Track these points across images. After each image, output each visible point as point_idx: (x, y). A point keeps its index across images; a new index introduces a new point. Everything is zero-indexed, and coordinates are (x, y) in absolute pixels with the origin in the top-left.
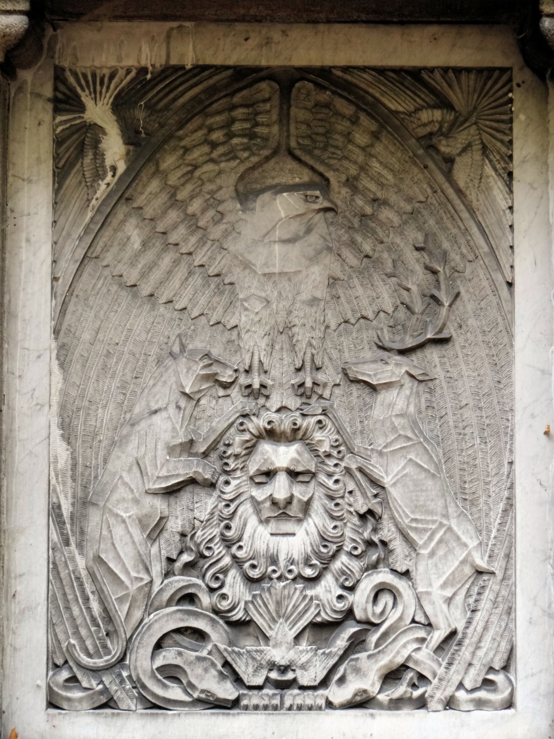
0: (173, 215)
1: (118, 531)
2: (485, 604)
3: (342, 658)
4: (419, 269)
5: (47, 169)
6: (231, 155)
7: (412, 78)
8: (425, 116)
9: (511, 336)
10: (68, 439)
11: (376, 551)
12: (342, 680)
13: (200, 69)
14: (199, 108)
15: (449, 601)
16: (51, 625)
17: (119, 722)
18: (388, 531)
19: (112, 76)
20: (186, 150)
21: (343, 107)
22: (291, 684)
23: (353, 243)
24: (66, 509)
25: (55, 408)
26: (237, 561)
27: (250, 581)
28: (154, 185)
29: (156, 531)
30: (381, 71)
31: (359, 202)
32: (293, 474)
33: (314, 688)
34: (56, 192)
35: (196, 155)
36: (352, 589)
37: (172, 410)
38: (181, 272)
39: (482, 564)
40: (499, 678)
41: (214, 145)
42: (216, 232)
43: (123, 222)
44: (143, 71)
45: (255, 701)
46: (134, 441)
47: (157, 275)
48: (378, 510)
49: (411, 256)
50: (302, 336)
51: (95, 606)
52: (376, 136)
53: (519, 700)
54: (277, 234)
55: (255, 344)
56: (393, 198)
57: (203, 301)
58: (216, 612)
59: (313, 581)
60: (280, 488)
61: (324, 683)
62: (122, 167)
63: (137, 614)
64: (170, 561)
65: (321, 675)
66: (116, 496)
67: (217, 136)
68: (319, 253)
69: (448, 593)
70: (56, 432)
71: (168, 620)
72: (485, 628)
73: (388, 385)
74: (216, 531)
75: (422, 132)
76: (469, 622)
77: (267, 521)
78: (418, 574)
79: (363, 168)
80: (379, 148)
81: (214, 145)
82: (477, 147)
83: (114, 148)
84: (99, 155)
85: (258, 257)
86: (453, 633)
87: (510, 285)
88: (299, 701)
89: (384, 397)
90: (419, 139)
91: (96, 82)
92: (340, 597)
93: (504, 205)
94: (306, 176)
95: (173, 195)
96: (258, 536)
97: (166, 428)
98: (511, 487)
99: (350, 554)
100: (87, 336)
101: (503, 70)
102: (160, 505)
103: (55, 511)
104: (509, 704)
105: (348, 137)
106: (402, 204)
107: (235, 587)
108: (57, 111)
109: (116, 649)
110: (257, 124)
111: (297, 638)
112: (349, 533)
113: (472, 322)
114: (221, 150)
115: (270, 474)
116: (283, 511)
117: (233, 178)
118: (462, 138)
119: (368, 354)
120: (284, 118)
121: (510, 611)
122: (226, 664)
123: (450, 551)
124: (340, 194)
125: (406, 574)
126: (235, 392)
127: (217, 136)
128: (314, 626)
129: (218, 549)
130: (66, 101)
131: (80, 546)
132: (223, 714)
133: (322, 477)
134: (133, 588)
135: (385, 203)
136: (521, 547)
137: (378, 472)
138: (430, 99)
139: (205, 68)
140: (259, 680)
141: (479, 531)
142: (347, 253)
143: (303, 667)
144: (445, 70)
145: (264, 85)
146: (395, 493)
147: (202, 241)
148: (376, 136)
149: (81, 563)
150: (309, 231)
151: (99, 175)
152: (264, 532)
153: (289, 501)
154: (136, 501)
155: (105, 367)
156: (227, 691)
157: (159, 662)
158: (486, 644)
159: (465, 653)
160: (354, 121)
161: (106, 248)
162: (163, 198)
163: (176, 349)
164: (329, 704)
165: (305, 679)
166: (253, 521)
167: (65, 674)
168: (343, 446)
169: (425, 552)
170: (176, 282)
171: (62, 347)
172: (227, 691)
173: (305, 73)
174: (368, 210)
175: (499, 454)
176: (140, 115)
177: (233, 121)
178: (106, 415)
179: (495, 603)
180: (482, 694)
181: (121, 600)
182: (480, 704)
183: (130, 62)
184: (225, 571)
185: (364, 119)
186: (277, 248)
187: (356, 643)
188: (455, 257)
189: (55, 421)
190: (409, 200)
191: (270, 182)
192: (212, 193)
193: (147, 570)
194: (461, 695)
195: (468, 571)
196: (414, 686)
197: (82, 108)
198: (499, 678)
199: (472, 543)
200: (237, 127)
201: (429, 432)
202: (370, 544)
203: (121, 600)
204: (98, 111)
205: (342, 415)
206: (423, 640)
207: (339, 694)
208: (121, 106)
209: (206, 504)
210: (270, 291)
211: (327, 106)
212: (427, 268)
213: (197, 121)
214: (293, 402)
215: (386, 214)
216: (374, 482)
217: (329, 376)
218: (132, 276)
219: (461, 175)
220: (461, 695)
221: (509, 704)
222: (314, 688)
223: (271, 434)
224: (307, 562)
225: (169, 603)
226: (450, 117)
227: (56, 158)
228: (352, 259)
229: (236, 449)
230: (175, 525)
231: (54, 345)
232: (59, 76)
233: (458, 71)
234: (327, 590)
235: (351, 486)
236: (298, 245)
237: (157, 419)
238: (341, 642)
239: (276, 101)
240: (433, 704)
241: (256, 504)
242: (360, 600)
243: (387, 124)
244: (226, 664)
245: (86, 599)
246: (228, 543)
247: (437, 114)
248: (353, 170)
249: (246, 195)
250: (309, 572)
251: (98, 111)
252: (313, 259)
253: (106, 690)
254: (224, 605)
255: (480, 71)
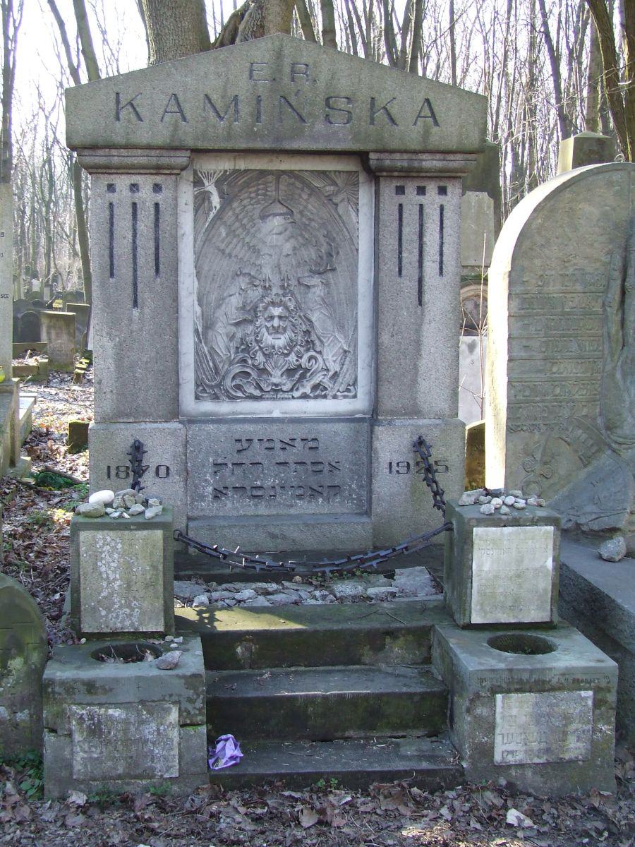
0: (237, 224)
1: (219, 338)
2: (347, 362)
3: (297, 382)
4: (325, 244)
5: (191, 207)
6: (258, 202)
7: (323, 174)
8: (327, 188)
9: (357, 268)
10: (200, 305)
11: (309, 345)
12: (297, 389)
13: (246, 171)
14: (247, 185)
15: (334, 361)
16: (196, 371)
17: (221, 404)
18: (313, 337)
19: (215, 173)
20: (242, 200)
21: (298, 184)
22: (281, 390)
23: (301, 235)
24: (200, 330)
25: (196, 295)
26: (261, 348)
27: (265, 355)
28: (230, 213)
29: (232, 338)
30: (312, 172)
31: (304, 220)
32: (280, 317)
33: (288, 392)
34: (195, 216)
35: (245, 202)
36: (301, 358)
37: (237, 295)
38: (240, 244)
39: (346, 349)
40: (352, 388)
41: (252, 199)
42: (252, 230)
43: (219, 227)
44: (226, 171)
45: (267, 396)
46: (223, 307)
47: (231, 246)
48: (310, 330)
49: (322, 240)
50: (283, 268)
51: (211, 364)
52: (310, 195)
53: (359, 395)
54: (274, 232)
55: (267, 272)
56: (316, 218)
57: (248, 255)
58: (253, 365)
59: (287, 355)
60: (276, 322)
61: (292, 390)
62: (218, 207)
63: (226, 367)
64: (237, 348)
65: (290, 387)
66: (218, 326)
67: (253, 195)
68: (289, 238)
69: (334, 359)
70: (196, 303)
71: (237, 369)
72: (347, 371)
73: (314, 286)
74: (253, 338)
75: (326, 194)
76: (341, 368)
77: (271, 334)
78: (324, 352)
79: (306, 207)
80: (311, 200)
81: (252, 199)
82: (346, 200)
83: (216, 200)
84: (210, 203)
85: (268, 239)
86: (336, 372)
87: (357, 250)
88: (282, 396)
89: (313, 290)
90: (326, 196)
91: (208, 175)
92: (297, 360)
93: (355, 221)
94: (285, 210)
95: (237, 217)
96: (268, 339)
97: (235, 301)
98: (357, 322)
99: (300, 345)
100: (206, 268)
101: (356, 172)
102: (234, 329)
103: (196, 331)
104: (355, 396)
105: (300, 196)
106: (319, 221)
107: (260, 358)
108: (194, 186)
109: (218, 379)
110: (267, 191)
111: (282, 375)
112: (299, 338)
113: (343, 263)
114: (254, 201)
115: (272, 318)
116: (276, 331)
117: (259, 211)
118: (340, 197)
119: (307, 274)
120: (277, 189)
121: (356, 364)
122: (257, 384)
123: (336, 344)
124: (297, 216)
125: (320, 353)
126: (259, 288)
127: (253, 195)
128: (288, 370)
129: (254, 344)
130: (198, 182)
131: (206, 343)
132: (296, 413)
133: (291, 319)
134: (224, 358)
135: (313, 220)
136: (359, 343)
137: (310, 316)
138: (330, 182)
139: (248, 170)
140: (269, 389)
141: (345, 337)
142: (300, 238)
143: (284, 385)
144: (335, 171)
145: (270, 177)
146: (316, 324)
147: (248, 233)
148: (310, 195)
149: (206, 349)
150: (286, 230)
151: (210, 209)
152: (270, 338)
153: (279, 327)
154: (225, 327)
155: (213, 279)
156: (257, 393)
157: (234, 383)
158: (347, 376)
159: (340, 379)
160: (302, 190)
161: (213, 236)
162: (233, 218)
163: (239, 273)
164: (293, 397)
165: (285, 388)
166: (266, 334)
167: (201, 388)
168: (298, 306)
169: (326, 344)
170: (238, 248)
171: (198, 273)
172: (257, 393)
173: (284, 172)
174: (307, 223)
175: (353, 311)
176: (225, 188)
177: (258, 189)
178: (213, 297)
179: (350, 362)
180: (346, 393)
181: (220, 362)
182: (345, 397)
183: (221, 168)
184: (256, 351)
185: (306, 189)
186: (275, 236)
187: (303, 376)
188: (338, 239)
189: (196, 299)
190: (322, 219)
191: (271, 212)
192: (251, 216)
193: (229, 351)
194: (339, 393)
195: (341, 351)
196: (322, 391)
197: (203, 185)
198: (352, 388)
199: (343, 341)
200: (260, 192)
201: (327, 303)
202: (307, 341)
203: (220, 362)
204: (210, 187)
205: (298, 297)
206: (325, 375)
207: (296, 394)
208: (218, 184)
209: (250, 328)
210: (272, 252)
211: (293, 184)
212: (327, 243)
213: (245, 190)
214: (281, 292)
215: (313, 224)
216: (309, 320)
217: (293, 282)
218: (223, 246)
219: (341, 210)
220: (339, 393)
221: (355, 396)
222: (288, 392)
223: (273, 304)
224: (285, 348)
225: (237, 363)
226: (337, 189)
227: (195, 203)
228: (301, 240)
229: (261, 309)
230: (239, 335)
231: (195, 272)
232: (195, 173)
233: (339, 172)
234: (292, 358)
235: (300, 321)
236: (282, 236)
237: (232, 298)
238: (297, 376)
239: (274, 182)
240: (329, 397)
241: (267, 328)
242: (304, 361)
243: (314, 191)
244: (257, 384)
245: (208, 362)
246: (257, 341)
247: (332, 188)
248: (301, 208)
249: (263, 217)
250: (286, 352)
251: (210, 187)
252: (287, 240)
253: (215, 394)
254: (256, 363)
255: (347, 172)
